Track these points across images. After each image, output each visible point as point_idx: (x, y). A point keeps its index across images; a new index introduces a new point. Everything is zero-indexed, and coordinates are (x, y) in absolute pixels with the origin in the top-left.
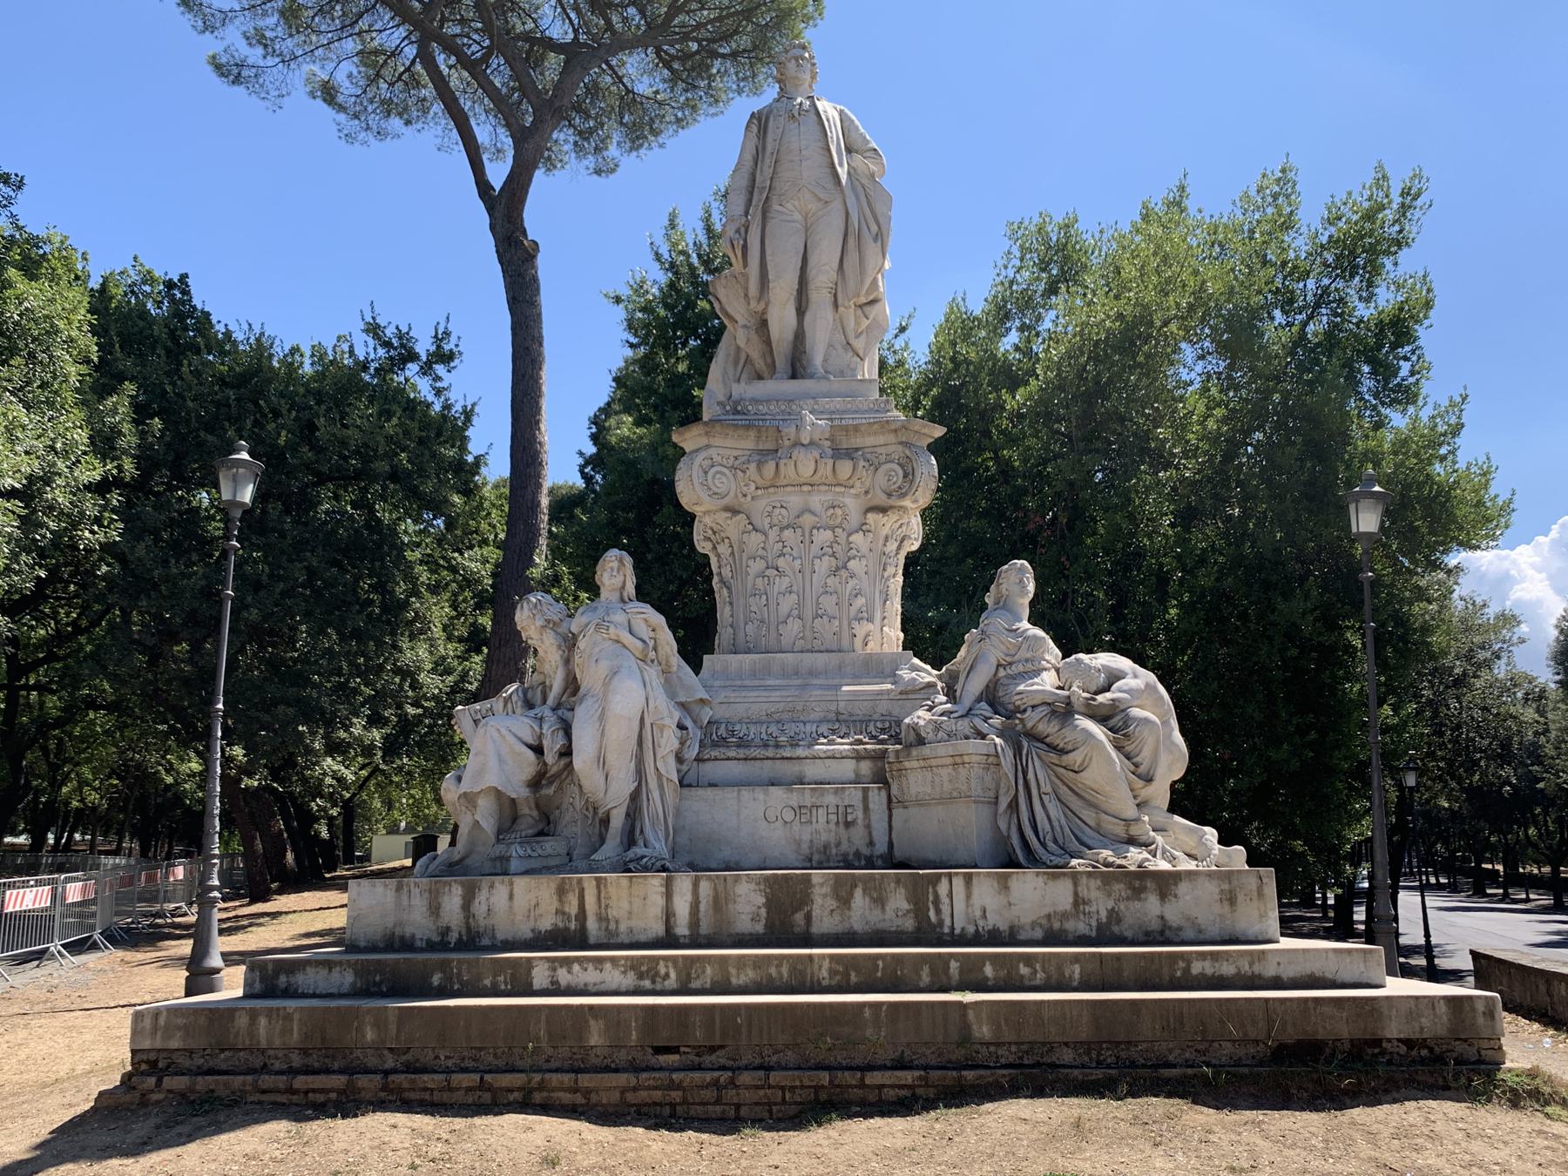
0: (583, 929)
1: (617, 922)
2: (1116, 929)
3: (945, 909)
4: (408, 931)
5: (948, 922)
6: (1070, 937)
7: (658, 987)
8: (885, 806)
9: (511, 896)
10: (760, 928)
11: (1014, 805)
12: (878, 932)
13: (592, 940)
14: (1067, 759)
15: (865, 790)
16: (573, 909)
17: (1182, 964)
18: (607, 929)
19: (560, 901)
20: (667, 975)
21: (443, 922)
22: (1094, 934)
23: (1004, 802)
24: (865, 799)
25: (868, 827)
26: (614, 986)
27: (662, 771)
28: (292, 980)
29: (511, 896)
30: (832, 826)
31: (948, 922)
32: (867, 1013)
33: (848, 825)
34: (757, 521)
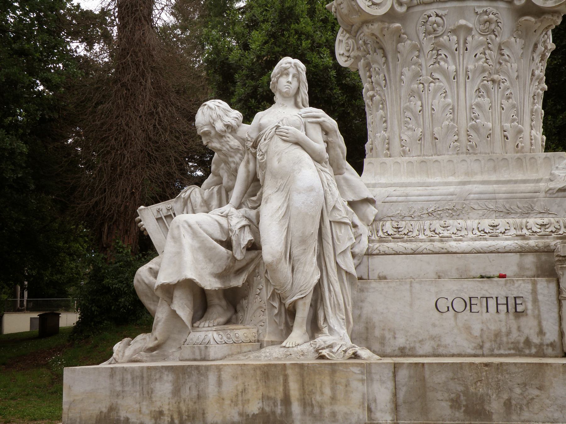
1: (321, 407)
4: (123, 414)
8: (554, 298)
9: (220, 383)
15: (534, 284)
16: (280, 396)
19: (267, 387)
21: (156, 407)
24: (534, 292)
25: (539, 318)
27: (343, 266)
29: (220, 383)
30: (503, 315)
33: (518, 314)
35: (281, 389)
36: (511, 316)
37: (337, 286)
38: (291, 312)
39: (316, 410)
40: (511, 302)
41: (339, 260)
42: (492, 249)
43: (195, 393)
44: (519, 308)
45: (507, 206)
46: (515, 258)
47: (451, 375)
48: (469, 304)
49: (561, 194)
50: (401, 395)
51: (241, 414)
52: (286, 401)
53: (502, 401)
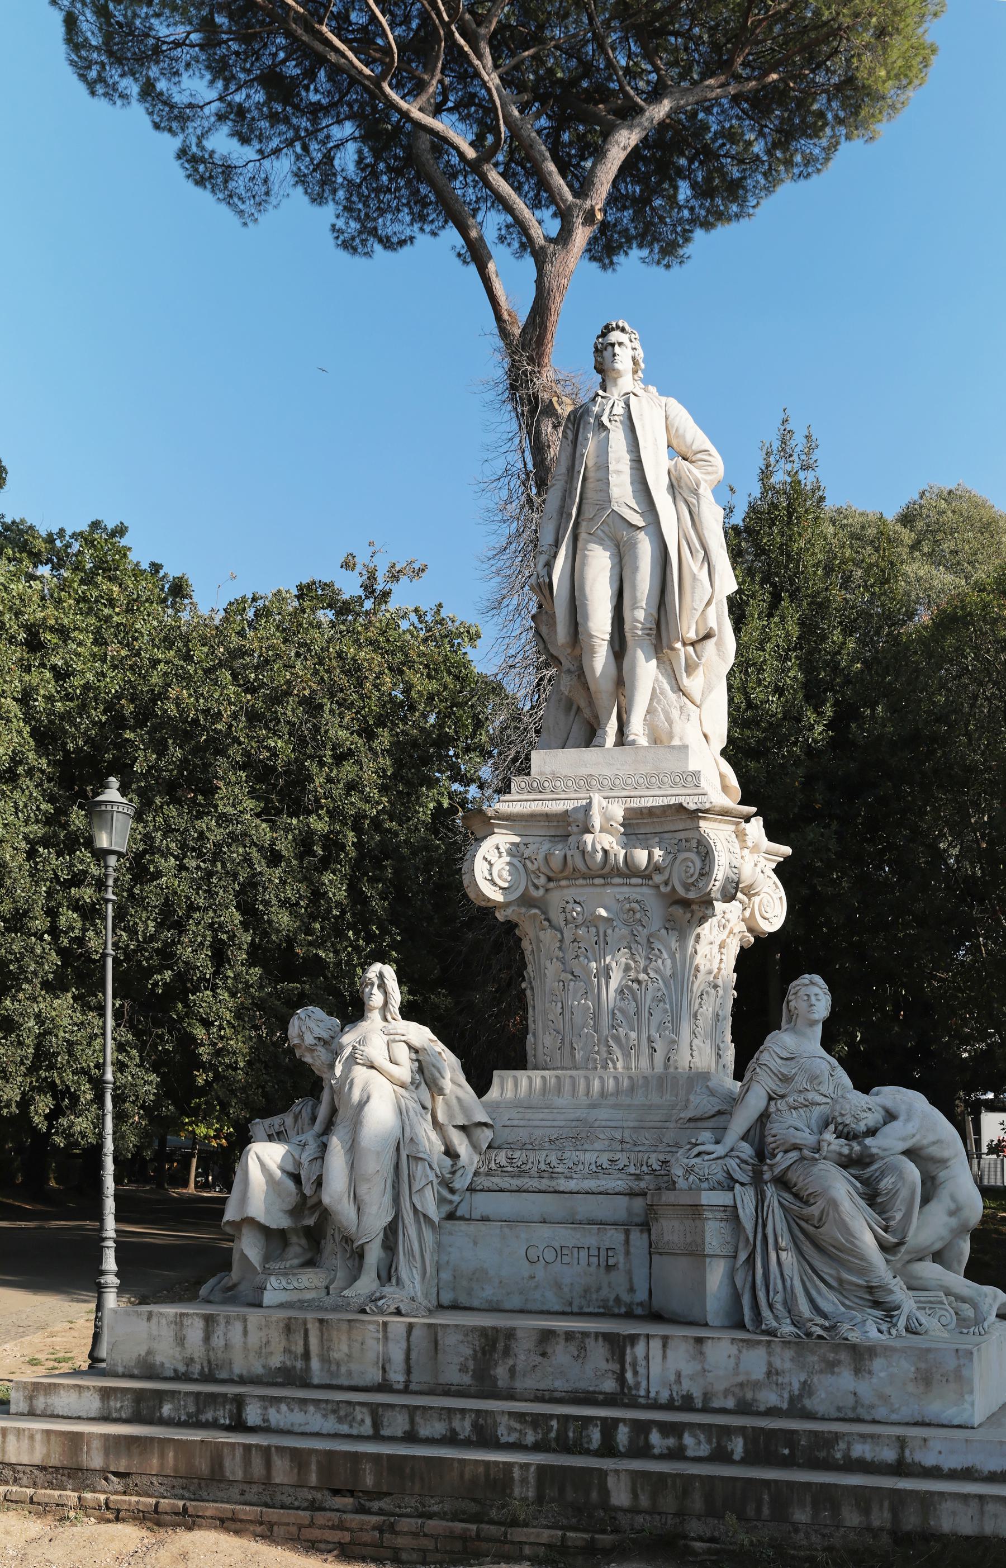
0: (308, 1369)
1: (338, 1365)
2: (807, 1403)
3: (642, 1370)
5: (644, 1384)
6: (762, 1408)
7: (355, 1432)
9: (245, 1332)
10: (467, 1379)
11: (751, 1259)
12: (576, 1391)
13: (316, 1381)
14: (807, 1211)
15: (627, 1233)
16: (300, 1349)
17: (842, 1445)
18: (329, 1370)
19: (288, 1339)
20: (363, 1421)
22: (785, 1406)
23: (743, 1256)
24: (627, 1241)
25: (629, 1273)
26: (316, 1429)
27: (419, 1207)
28: (49, 1401)
29: (245, 1332)
30: (593, 1269)
31: (644, 1384)
32: (516, 1473)
34: (553, 916)
35: (301, 1343)
36: (602, 1270)
37: (412, 1231)
38: (360, 1254)
39: (334, 1368)
40: (603, 1253)
41: (415, 1200)
42: (601, 1189)
43: (222, 1343)
44: (611, 1262)
45: (634, 1137)
46: (624, 1200)
47: (461, 1338)
48: (560, 1252)
49: (692, 1125)
50: (414, 1355)
51: (264, 1367)
52: (306, 1355)
53: (507, 1367)
